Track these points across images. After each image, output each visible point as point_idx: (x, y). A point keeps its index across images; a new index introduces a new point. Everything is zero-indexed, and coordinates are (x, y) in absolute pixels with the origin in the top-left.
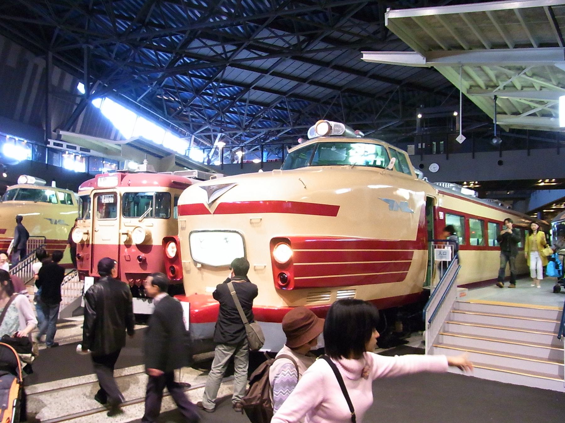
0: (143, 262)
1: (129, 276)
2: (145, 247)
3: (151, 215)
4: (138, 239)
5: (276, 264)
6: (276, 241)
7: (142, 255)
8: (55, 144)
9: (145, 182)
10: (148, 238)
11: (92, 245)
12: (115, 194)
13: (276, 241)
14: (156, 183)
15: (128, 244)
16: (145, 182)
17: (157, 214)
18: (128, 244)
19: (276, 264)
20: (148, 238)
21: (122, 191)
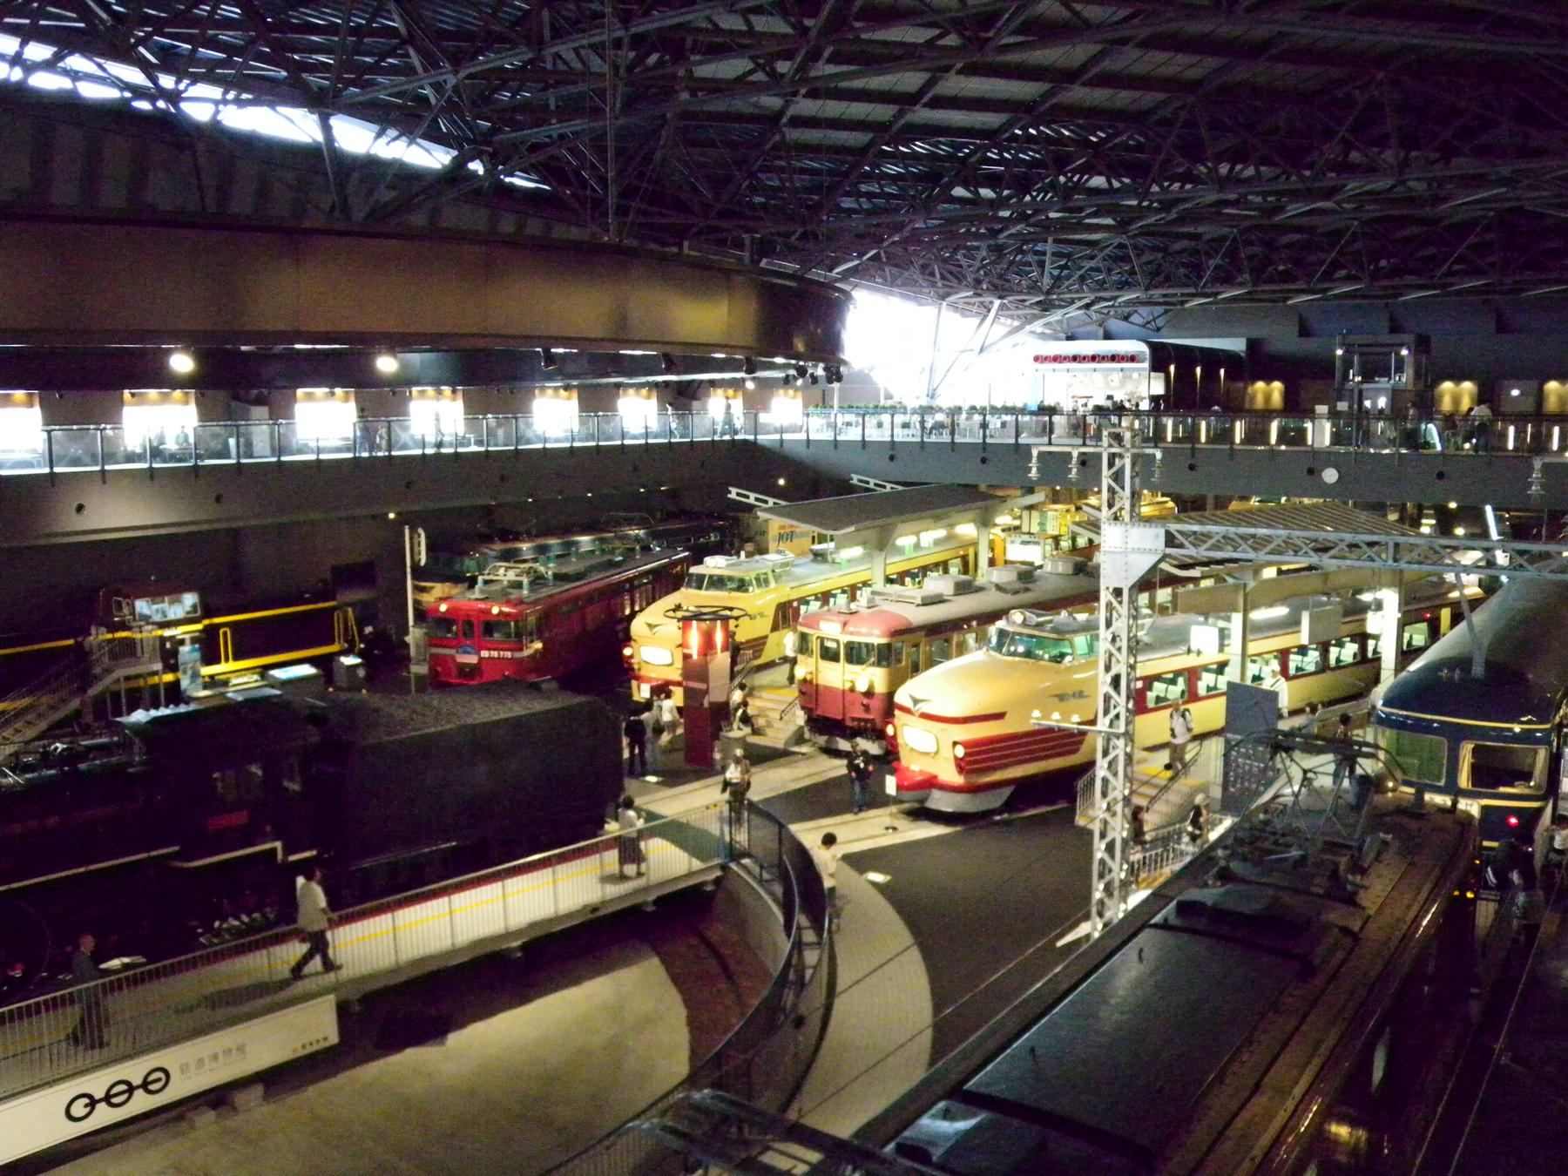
0: (867, 708)
1: (853, 719)
2: (869, 694)
3: (873, 664)
4: (862, 687)
5: (956, 759)
6: (955, 744)
7: (865, 701)
8: (738, 494)
9: (864, 630)
10: (871, 687)
11: (817, 685)
12: (838, 642)
13: (955, 744)
14: (877, 632)
15: (852, 690)
16: (864, 630)
17: (878, 664)
18: (852, 690)
19: (956, 759)
20: (871, 687)
21: (844, 639)
